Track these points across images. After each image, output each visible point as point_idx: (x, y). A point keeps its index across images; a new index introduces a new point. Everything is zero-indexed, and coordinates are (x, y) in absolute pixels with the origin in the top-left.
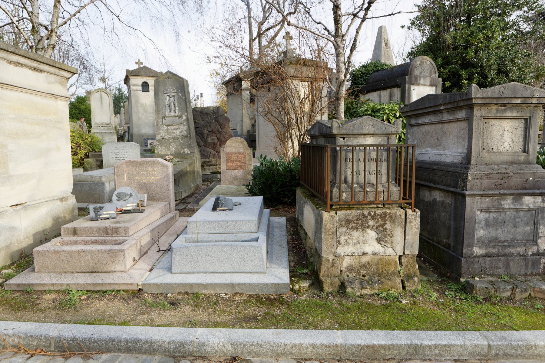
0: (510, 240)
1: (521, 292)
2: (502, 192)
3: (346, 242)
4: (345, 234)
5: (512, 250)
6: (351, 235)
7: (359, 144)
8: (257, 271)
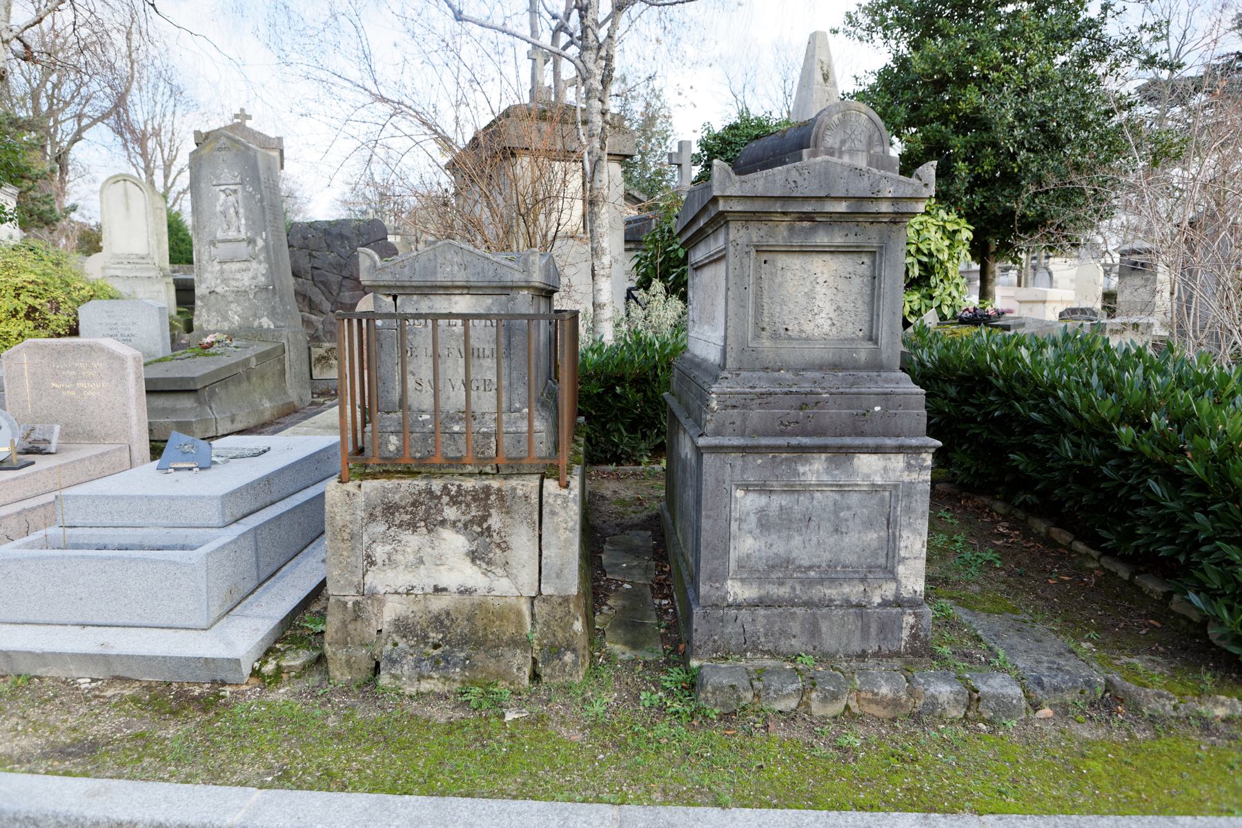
0: (824, 565)
1: (824, 700)
2: (794, 441)
3: (389, 559)
4: (385, 539)
5: (828, 592)
6: (400, 542)
7: (433, 311)
8: (187, 624)
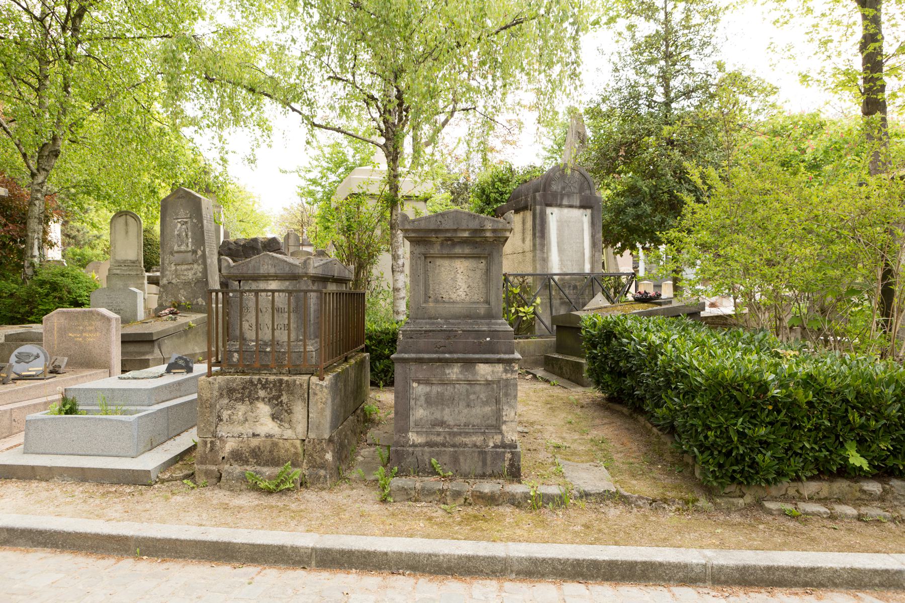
5: (464, 440)
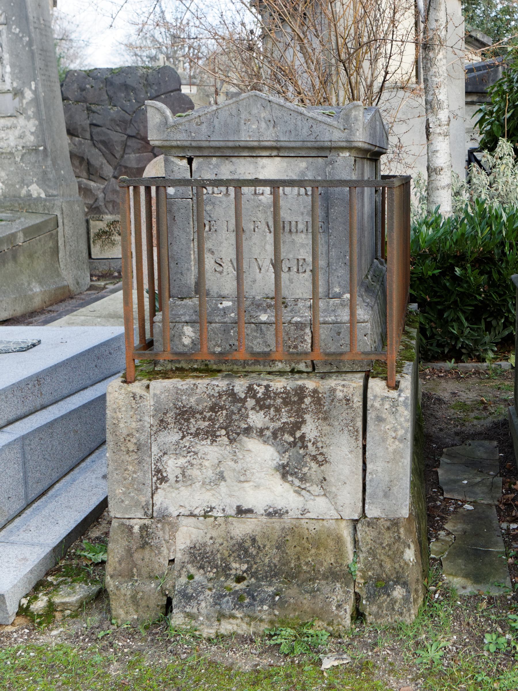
6: (196, 453)
7: (236, 177)
